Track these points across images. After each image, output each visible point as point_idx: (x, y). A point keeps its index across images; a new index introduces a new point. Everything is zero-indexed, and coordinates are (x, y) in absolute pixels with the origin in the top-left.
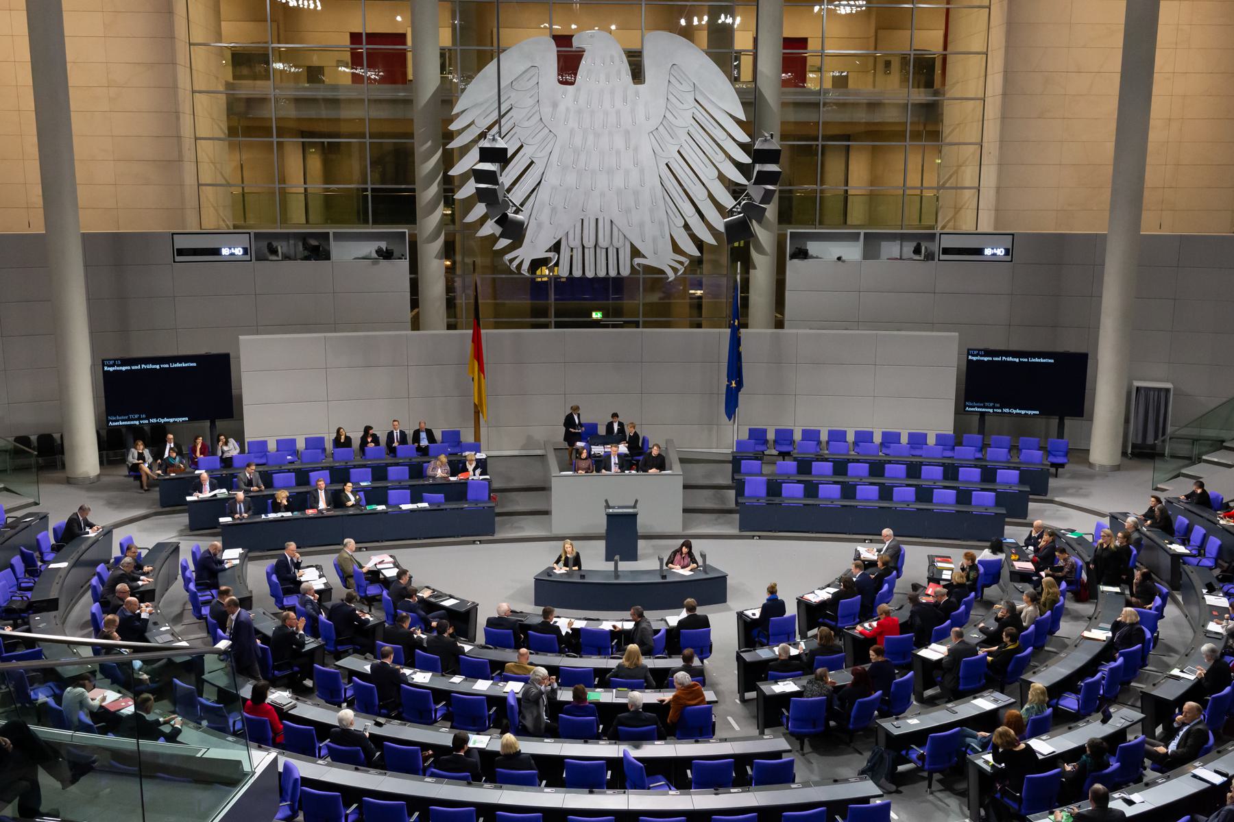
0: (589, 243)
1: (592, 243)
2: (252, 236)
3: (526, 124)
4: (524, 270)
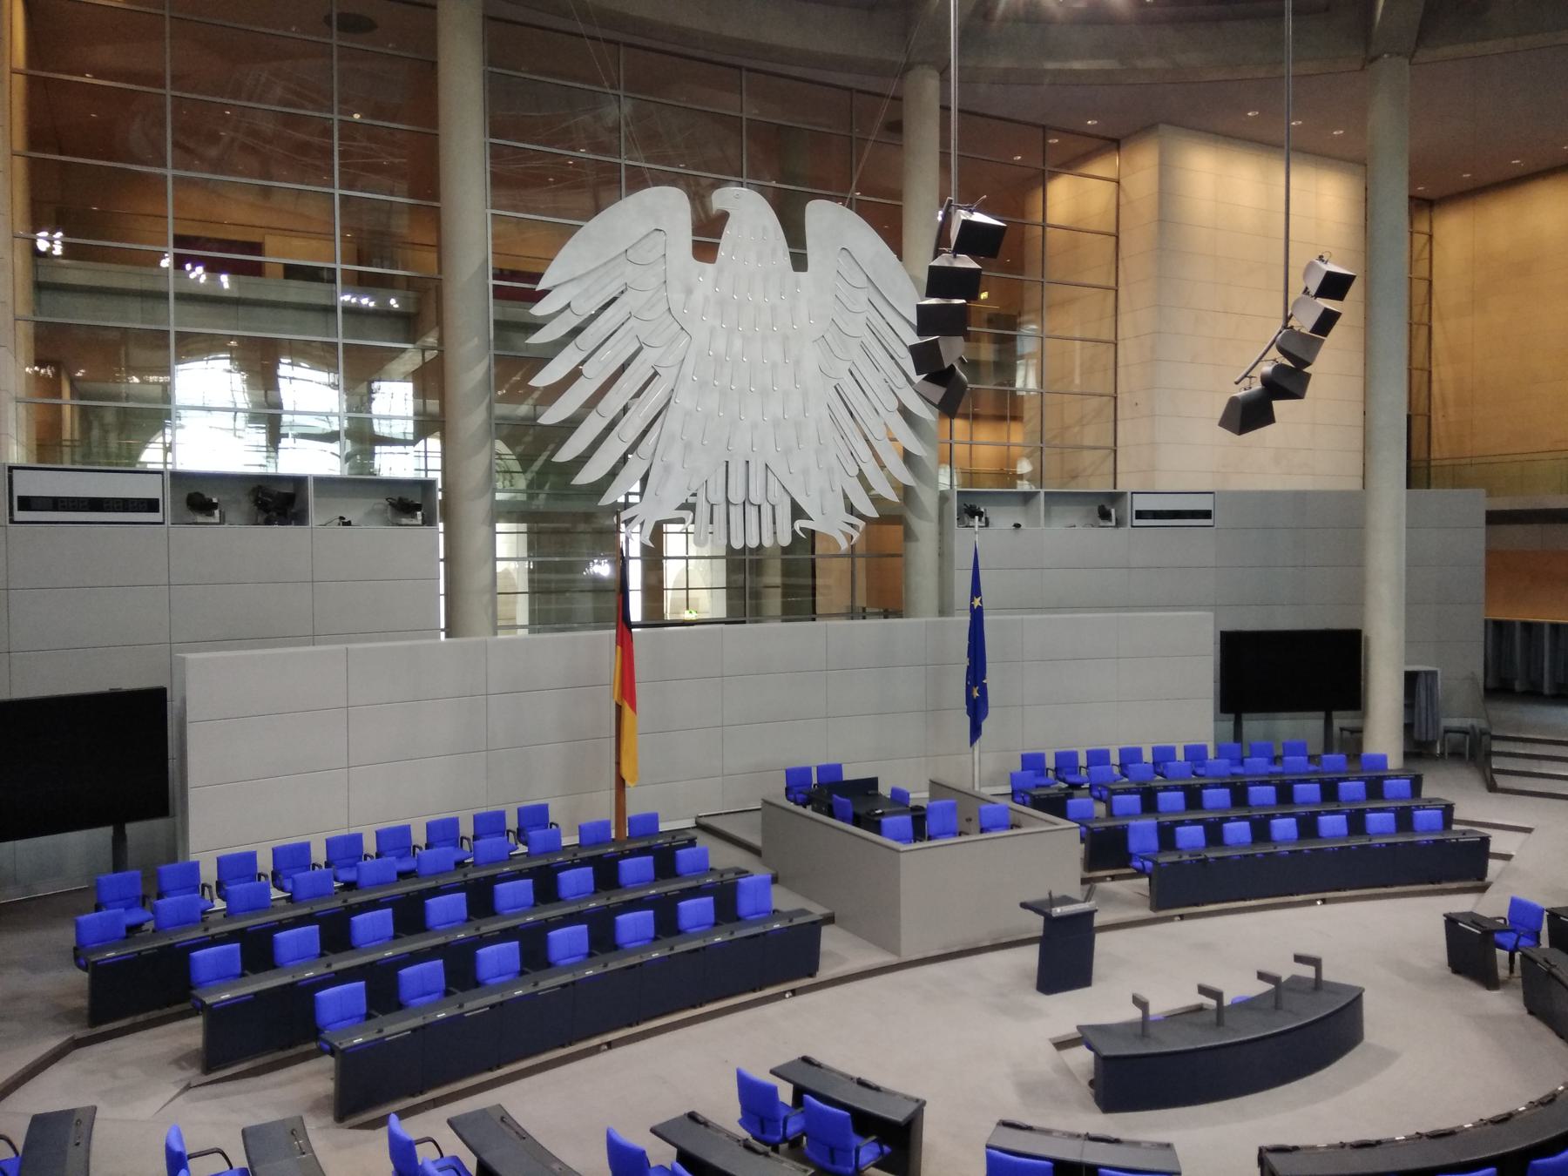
0: (737, 496)
2: (167, 476)
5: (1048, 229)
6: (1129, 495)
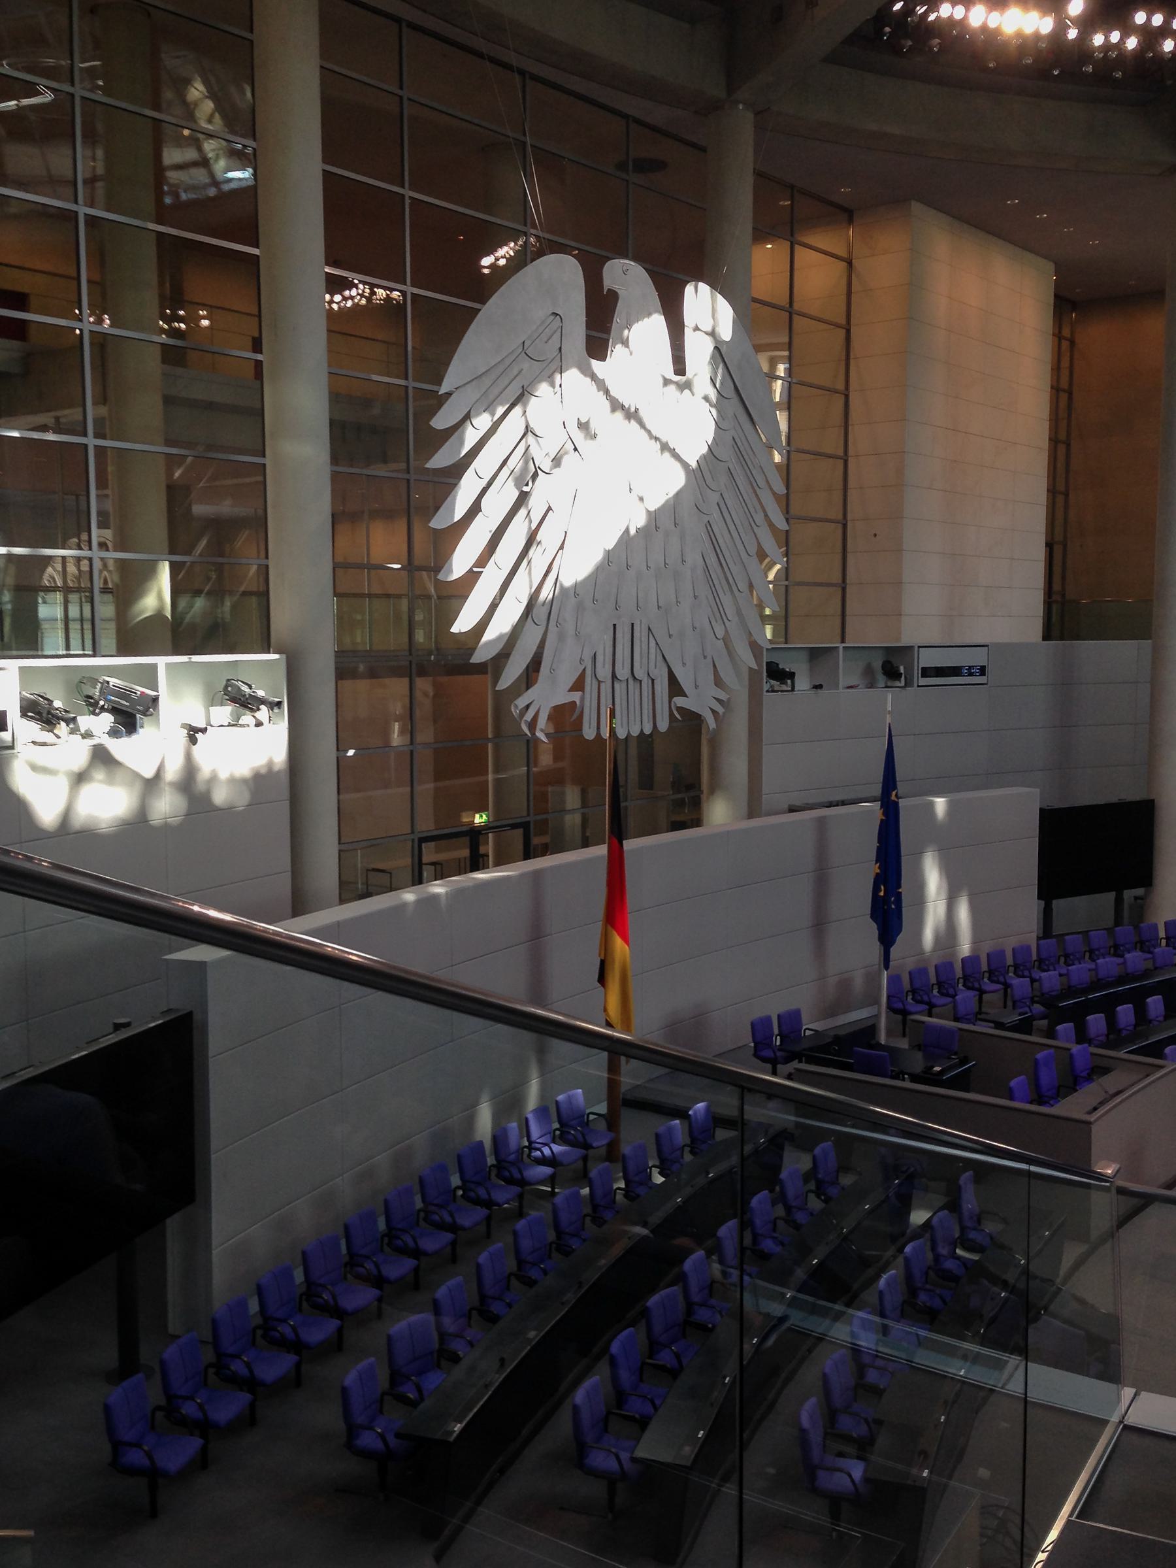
5: (796, 318)
6: (916, 649)
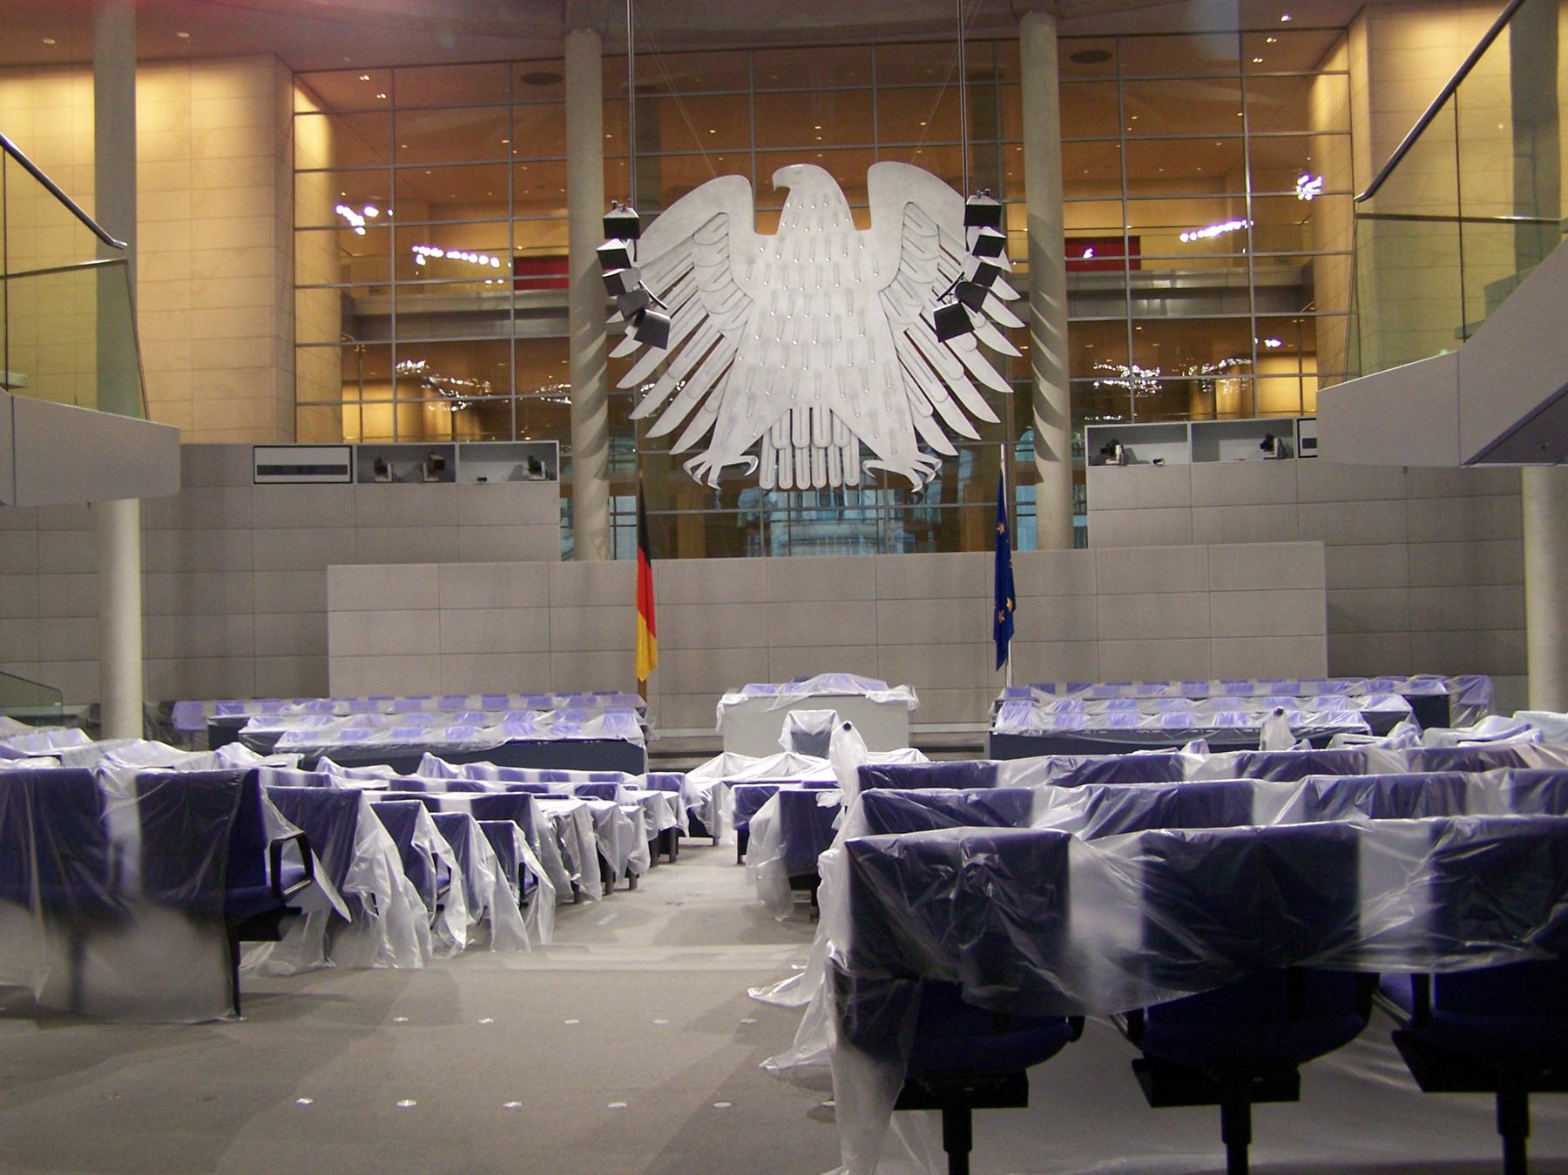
0: (801, 440)
1: (805, 442)
3: (714, 287)
4: (712, 481)
